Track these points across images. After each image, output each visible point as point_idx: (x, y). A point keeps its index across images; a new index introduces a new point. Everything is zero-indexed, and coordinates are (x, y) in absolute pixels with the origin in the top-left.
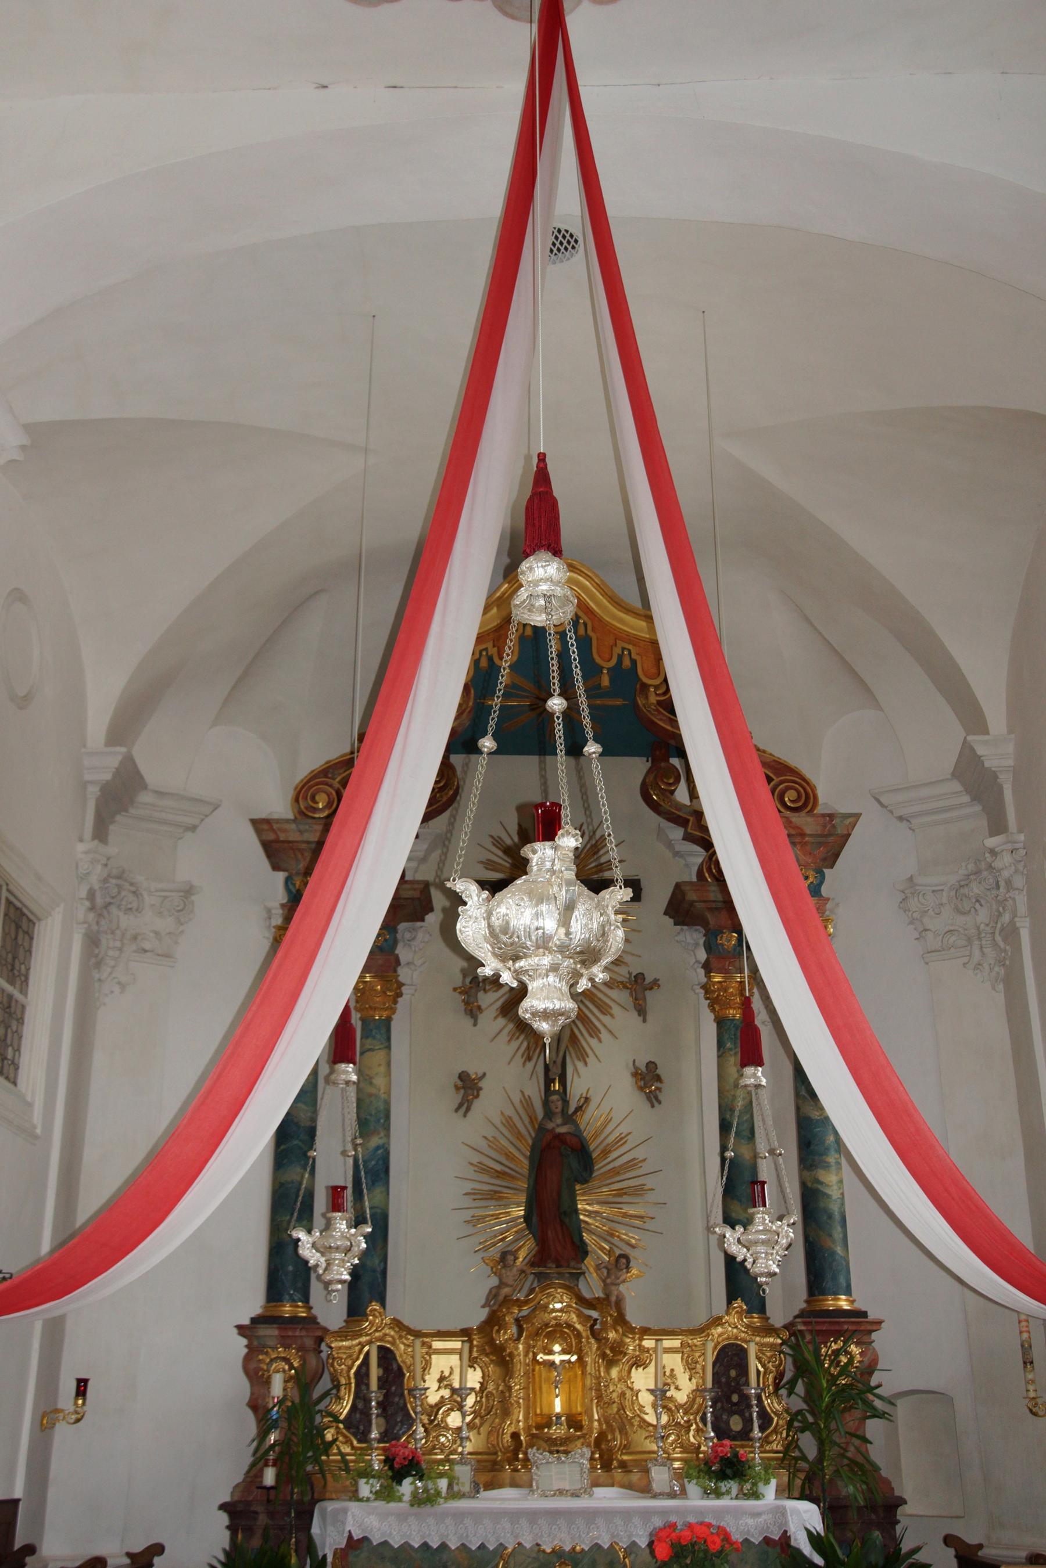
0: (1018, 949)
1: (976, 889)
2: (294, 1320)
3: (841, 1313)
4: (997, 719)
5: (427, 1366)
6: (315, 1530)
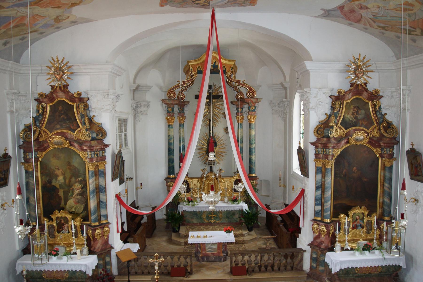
0: (287, 116)
1: (281, 104)
2: (173, 178)
3: (253, 177)
4: (288, 79)
5: (192, 183)
6: (178, 208)
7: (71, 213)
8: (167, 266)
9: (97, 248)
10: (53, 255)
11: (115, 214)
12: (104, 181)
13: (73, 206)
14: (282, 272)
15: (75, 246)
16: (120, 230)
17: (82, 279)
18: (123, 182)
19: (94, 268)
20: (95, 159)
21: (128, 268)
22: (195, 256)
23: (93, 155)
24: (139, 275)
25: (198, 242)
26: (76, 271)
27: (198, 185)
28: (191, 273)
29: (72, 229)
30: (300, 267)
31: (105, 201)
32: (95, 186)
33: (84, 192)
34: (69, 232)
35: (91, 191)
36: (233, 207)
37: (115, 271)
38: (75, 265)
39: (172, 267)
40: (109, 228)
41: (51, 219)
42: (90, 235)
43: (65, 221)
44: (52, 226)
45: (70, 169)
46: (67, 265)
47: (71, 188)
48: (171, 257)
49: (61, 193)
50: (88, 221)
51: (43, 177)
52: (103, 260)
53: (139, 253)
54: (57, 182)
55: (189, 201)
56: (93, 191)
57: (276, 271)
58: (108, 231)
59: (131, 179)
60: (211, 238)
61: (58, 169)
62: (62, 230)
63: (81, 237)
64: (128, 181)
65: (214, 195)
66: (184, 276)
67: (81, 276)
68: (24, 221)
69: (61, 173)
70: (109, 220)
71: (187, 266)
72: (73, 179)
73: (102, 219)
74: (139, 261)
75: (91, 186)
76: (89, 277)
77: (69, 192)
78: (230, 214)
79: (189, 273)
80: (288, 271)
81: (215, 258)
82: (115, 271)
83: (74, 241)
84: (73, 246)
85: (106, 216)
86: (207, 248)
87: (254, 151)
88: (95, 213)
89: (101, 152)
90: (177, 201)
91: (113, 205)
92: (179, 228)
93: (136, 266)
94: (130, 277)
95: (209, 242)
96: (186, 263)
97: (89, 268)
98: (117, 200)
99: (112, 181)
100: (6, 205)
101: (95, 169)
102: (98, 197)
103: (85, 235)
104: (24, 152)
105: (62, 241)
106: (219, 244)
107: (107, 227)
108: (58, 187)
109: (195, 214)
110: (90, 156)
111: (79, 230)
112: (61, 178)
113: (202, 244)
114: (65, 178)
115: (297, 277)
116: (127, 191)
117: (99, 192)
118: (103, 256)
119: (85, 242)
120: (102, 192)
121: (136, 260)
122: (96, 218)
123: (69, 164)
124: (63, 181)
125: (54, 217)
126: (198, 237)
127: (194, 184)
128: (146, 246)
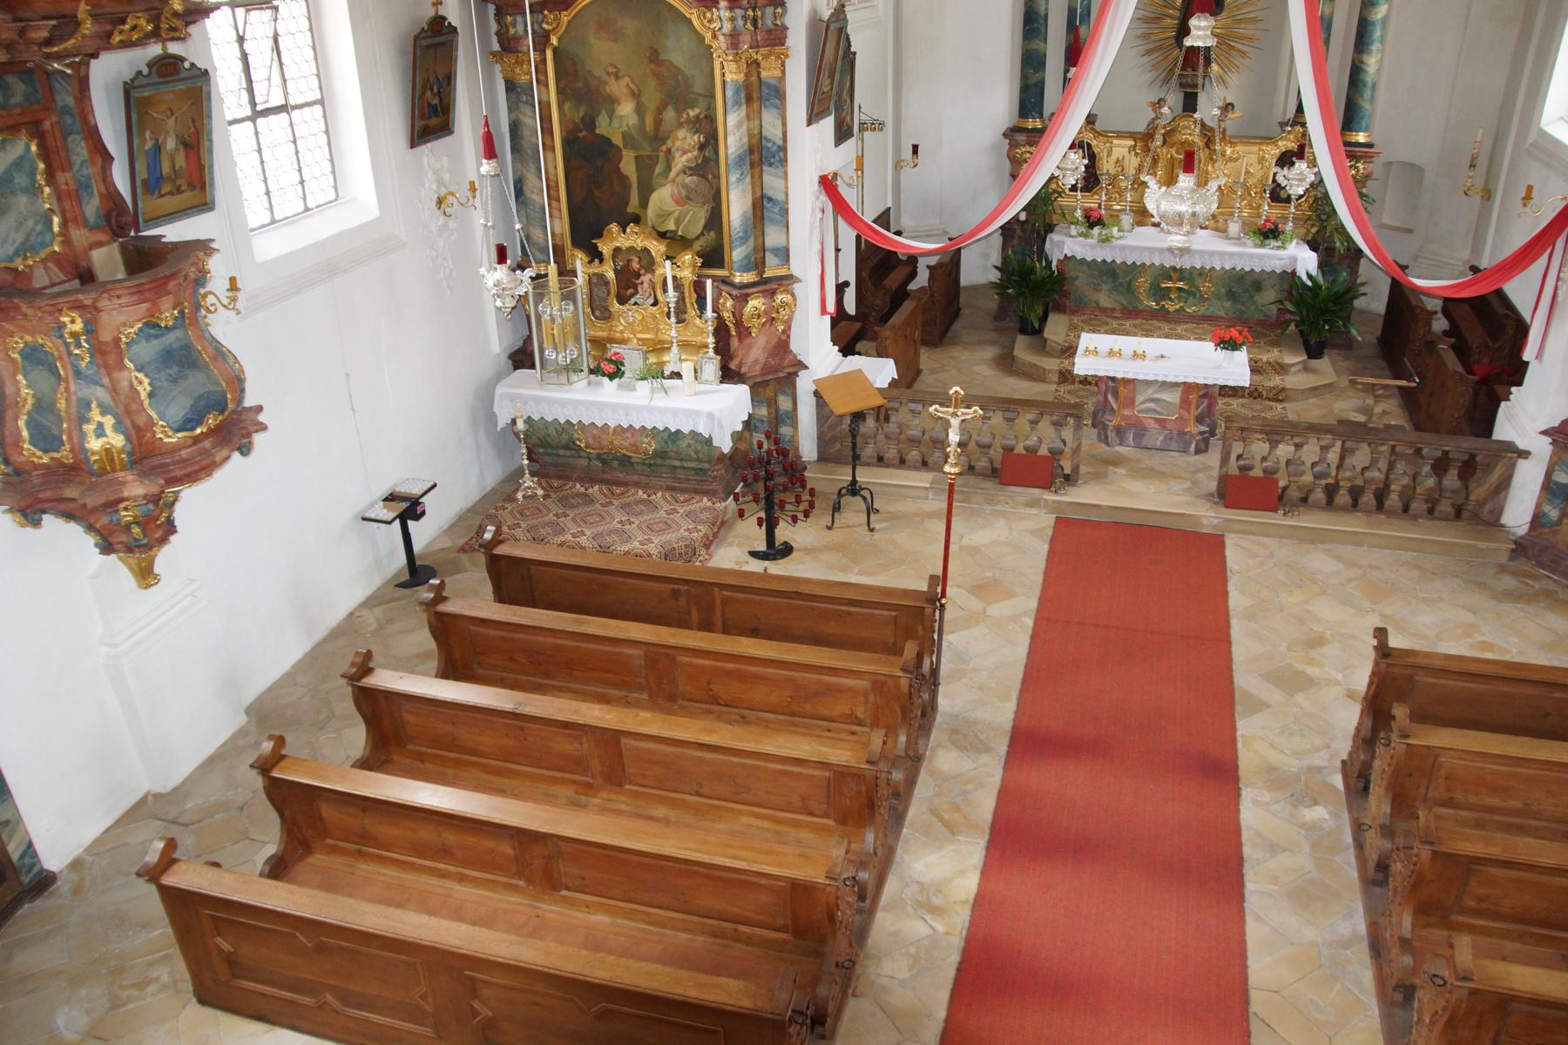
2: (1035, 130)
3: (1358, 144)
5: (1109, 154)
6: (1047, 246)
7: (662, 235)
8: (989, 446)
9: (749, 360)
10: (604, 375)
11: (817, 247)
12: (779, 123)
13: (670, 213)
14: (1415, 518)
15: (675, 349)
16: (831, 307)
17: (698, 460)
18: (849, 134)
19: (739, 427)
20: (748, 38)
21: (854, 437)
22: (1094, 426)
23: (740, 22)
24: (888, 466)
25: (1111, 374)
26: (678, 431)
27: (1132, 162)
28: (1070, 480)
29: (665, 291)
30: (1491, 512)
31: (781, 197)
32: (746, 140)
33: (706, 160)
34: (655, 303)
35: (731, 157)
36: (1261, 257)
37: (808, 448)
38: (675, 412)
39: (1009, 450)
40: (793, 295)
41: (595, 255)
42: (726, 315)
43: (644, 262)
44: (601, 277)
45: (657, 75)
46: (650, 409)
47: (664, 148)
48: (1008, 415)
49: (628, 166)
50: (721, 265)
51: (567, 106)
52: (769, 407)
53: (895, 392)
54: (615, 124)
55: (1092, 221)
56: (741, 158)
57: (1390, 513)
58: (791, 306)
59: (877, 126)
60: (1161, 362)
61: (617, 78)
62: (632, 295)
63: (698, 321)
64: (867, 134)
65: (1193, 191)
66: (1047, 486)
67: (696, 452)
68: (509, 253)
69: (625, 90)
70: (795, 268)
71: (1061, 452)
72: (670, 114)
73: (771, 260)
74: (893, 419)
75: (731, 140)
76: (722, 457)
77: (653, 160)
78: (1242, 285)
79: (1067, 478)
80: (1439, 519)
81: (1169, 438)
82: (808, 448)
83: (673, 333)
84: (669, 349)
85: (784, 254)
86: (1140, 398)
87: (1377, 33)
88: (744, 239)
89: (769, 10)
90: (1043, 204)
91: (809, 211)
92: (1044, 320)
93: (880, 437)
94: (859, 470)
95: (1151, 378)
96: (1061, 445)
97: (721, 426)
98: (824, 198)
99: (809, 123)
100: (451, 199)
101: (747, 76)
102: (757, 182)
103: (709, 313)
104: (499, 15)
105: (633, 332)
106: (1188, 388)
107: (787, 291)
108: (617, 140)
109: (1109, 272)
110: (727, 27)
111: (691, 297)
112: (626, 109)
113: (1127, 382)
114: (640, 110)
115: (1468, 545)
116: (860, 167)
117: (761, 162)
118: (769, 392)
119: (711, 340)
120: (771, 165)
121: (882, 414)
122: (747, 257)
123: (654, 57)
124: (633, 120)
125: (605, 248)
126: (1111, 353)
127: (1114, 158)
128: (919, 372)
